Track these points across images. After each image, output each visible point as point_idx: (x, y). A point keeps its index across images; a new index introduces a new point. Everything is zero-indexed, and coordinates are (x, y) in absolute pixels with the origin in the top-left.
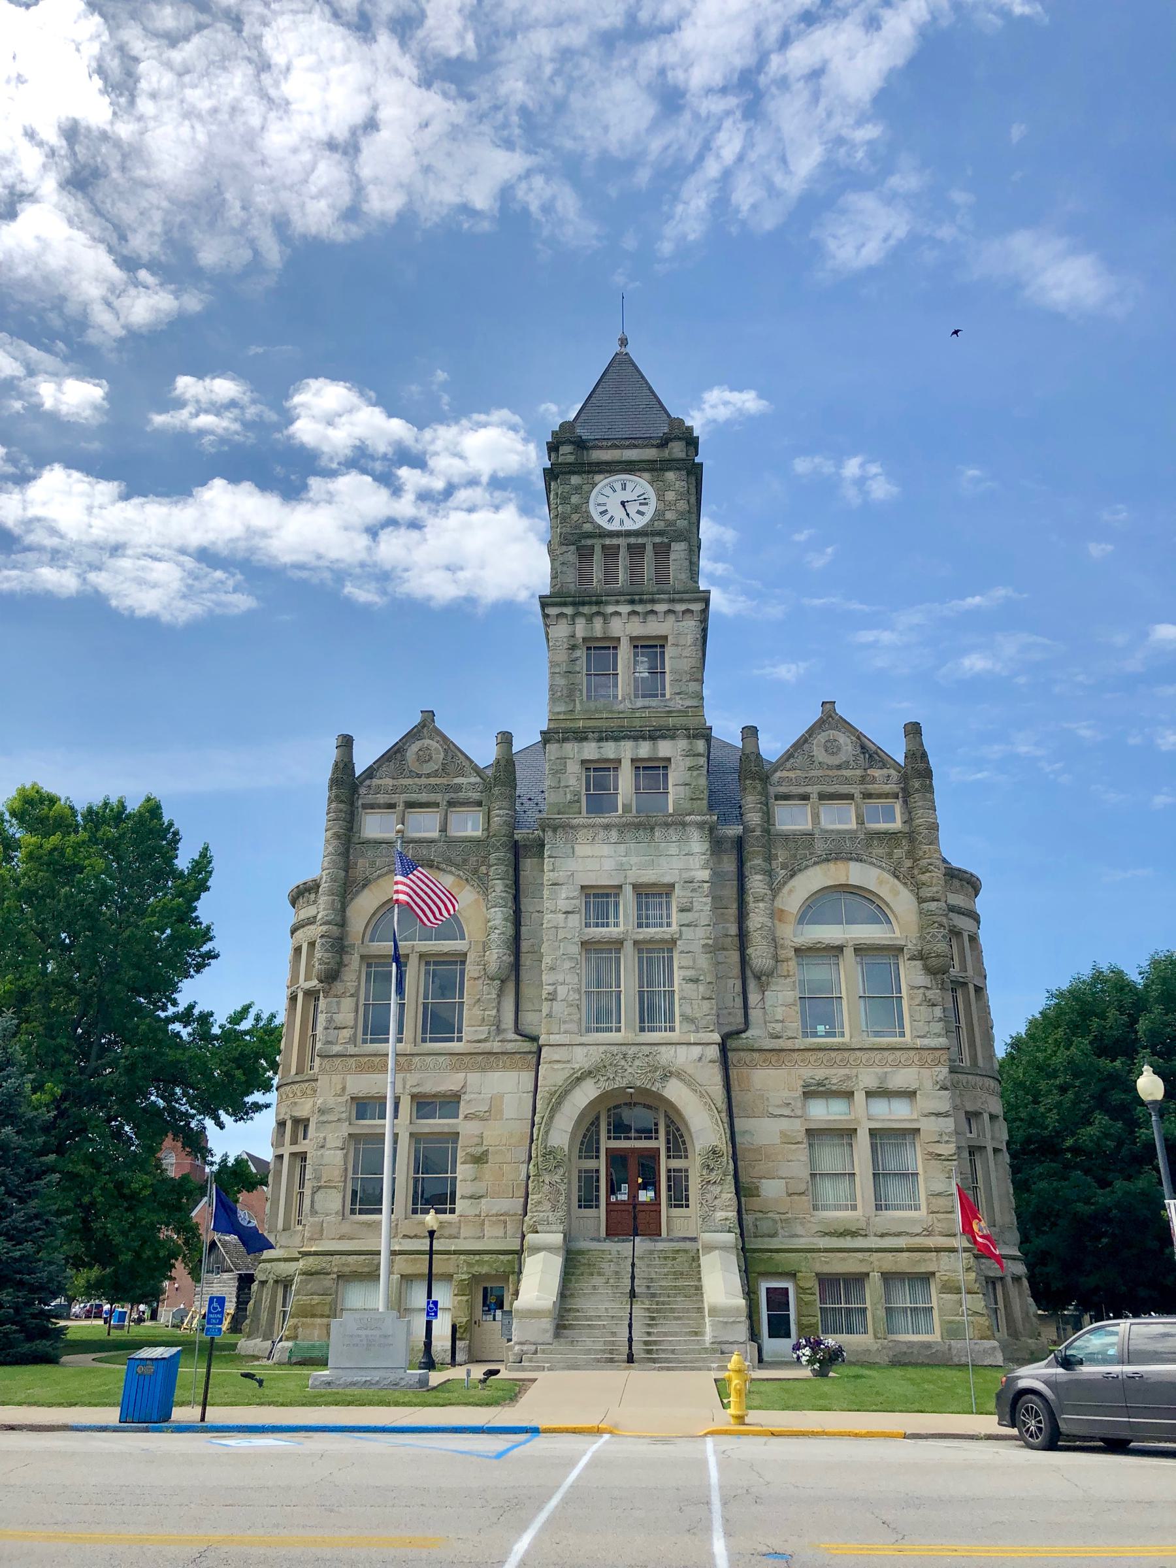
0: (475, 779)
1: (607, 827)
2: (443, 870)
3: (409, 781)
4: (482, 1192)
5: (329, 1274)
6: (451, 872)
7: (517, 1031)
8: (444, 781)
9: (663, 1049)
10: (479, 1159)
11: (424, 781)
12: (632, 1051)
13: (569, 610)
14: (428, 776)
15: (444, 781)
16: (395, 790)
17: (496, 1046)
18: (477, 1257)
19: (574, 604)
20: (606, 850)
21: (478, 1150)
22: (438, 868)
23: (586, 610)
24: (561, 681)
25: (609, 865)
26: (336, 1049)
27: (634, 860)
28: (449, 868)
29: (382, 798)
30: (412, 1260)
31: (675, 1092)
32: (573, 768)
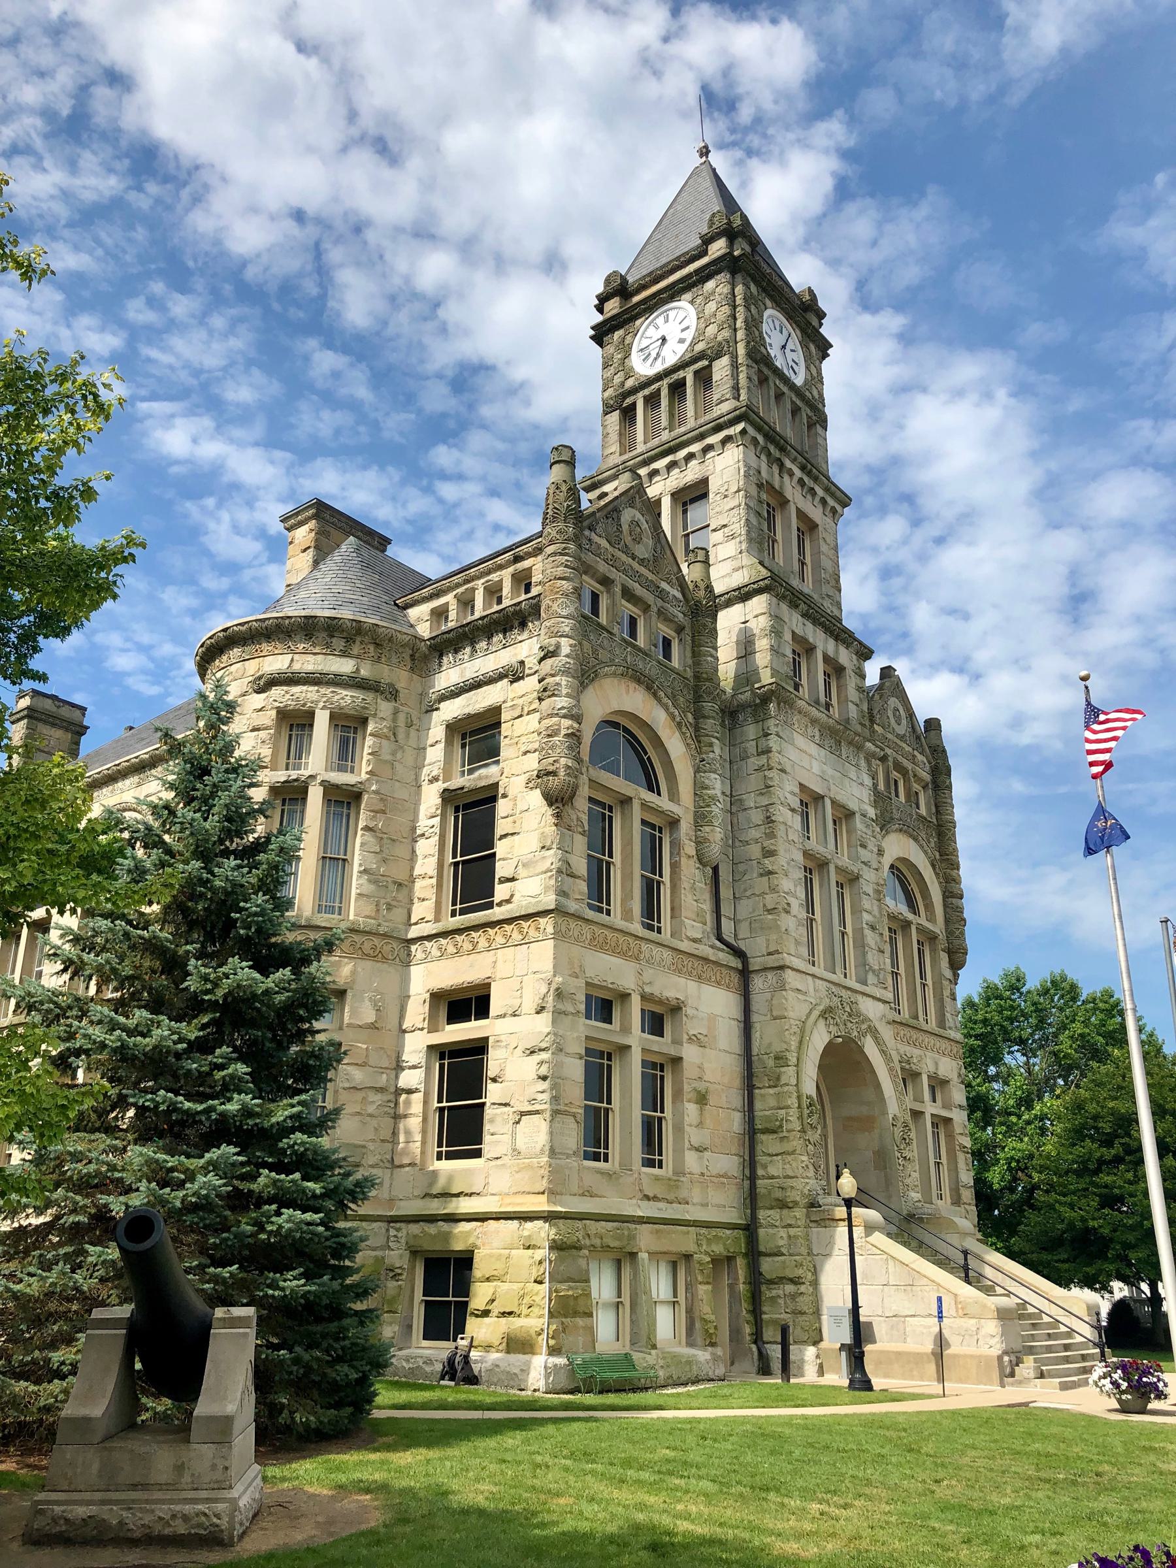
0: (679, 595)
1: (814, 721)
2: (659, 700)
3: (624, 557)
4: (707, 1142)
5: (579, 1248)
6: (667, 709)
7: (720, 938)
8: (651, 576)
9: (860, 998)
10: (702, 1099)
11: (635, 565)
12: (844, 993)
13: (760, 439)
14: (642, 562)
15: (651, 576)
16: (613, 562)
17: (705, 950)
18: (714, 1232)
19: (766, 436)
20: (813, 749)
21: (701, 1086)
22: (655, 695)
23: (772, 448)
24: (754, 521)
25: (816, 768)
26: (572, 906)
27: (830, 772)
28: (665, 700)
29: (603, 567)
30: (657, 1231)
31: (870, 1049)
32: (788, 636)
